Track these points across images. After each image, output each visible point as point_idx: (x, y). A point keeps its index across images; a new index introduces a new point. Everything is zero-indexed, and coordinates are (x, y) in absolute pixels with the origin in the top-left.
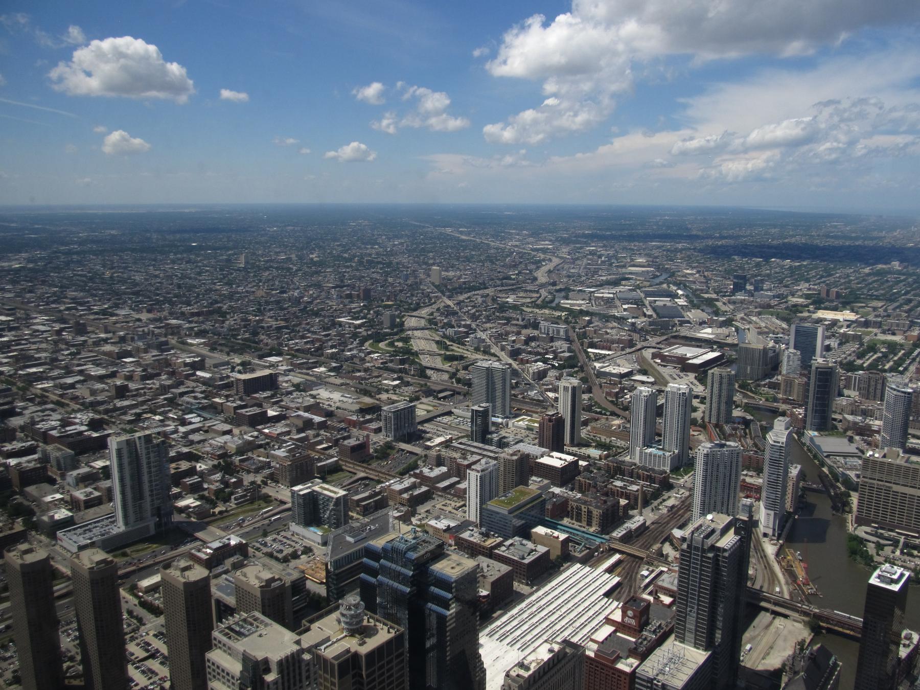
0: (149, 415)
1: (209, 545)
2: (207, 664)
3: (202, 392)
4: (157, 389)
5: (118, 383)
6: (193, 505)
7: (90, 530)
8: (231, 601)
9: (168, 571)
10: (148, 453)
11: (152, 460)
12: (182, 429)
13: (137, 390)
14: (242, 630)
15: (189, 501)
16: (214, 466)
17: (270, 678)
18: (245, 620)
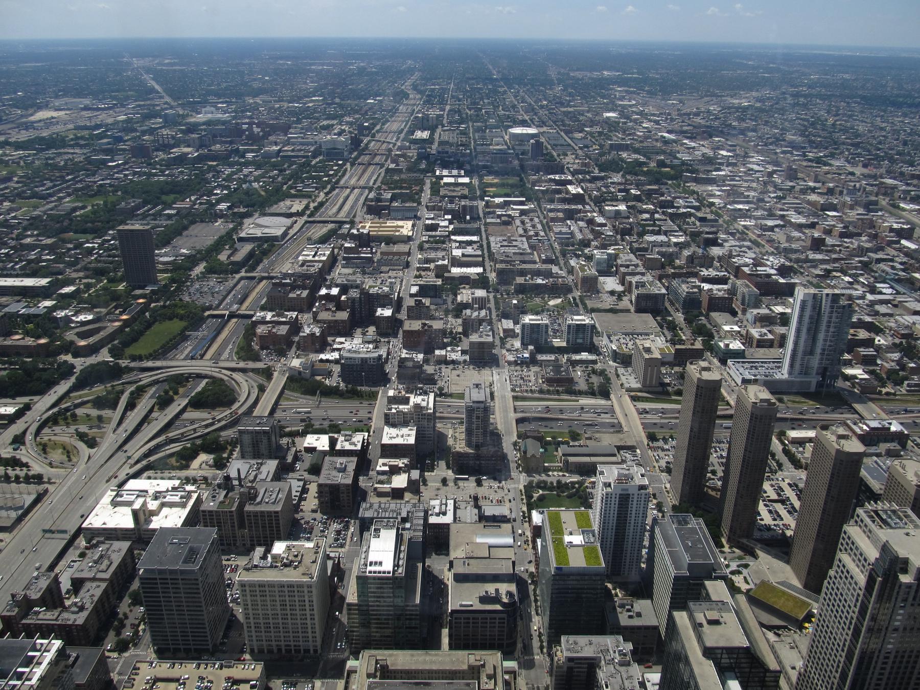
0: (839, 274)
1: (867, 422)
2: (843, 535)
3: (901, 263)
4: (854, 249)
5: (816, 235)
6: (860, 377)
7: (756, 368)
8: (876, 485)
9: (824, 432)
10: (831, 312)
11: (834, 319)
12: (870, 297)
13: (833, 246)
14: (889, 520)
15: (858, 372)
16: (894, 344)
17: (905, 579)
18: (894, 512)
